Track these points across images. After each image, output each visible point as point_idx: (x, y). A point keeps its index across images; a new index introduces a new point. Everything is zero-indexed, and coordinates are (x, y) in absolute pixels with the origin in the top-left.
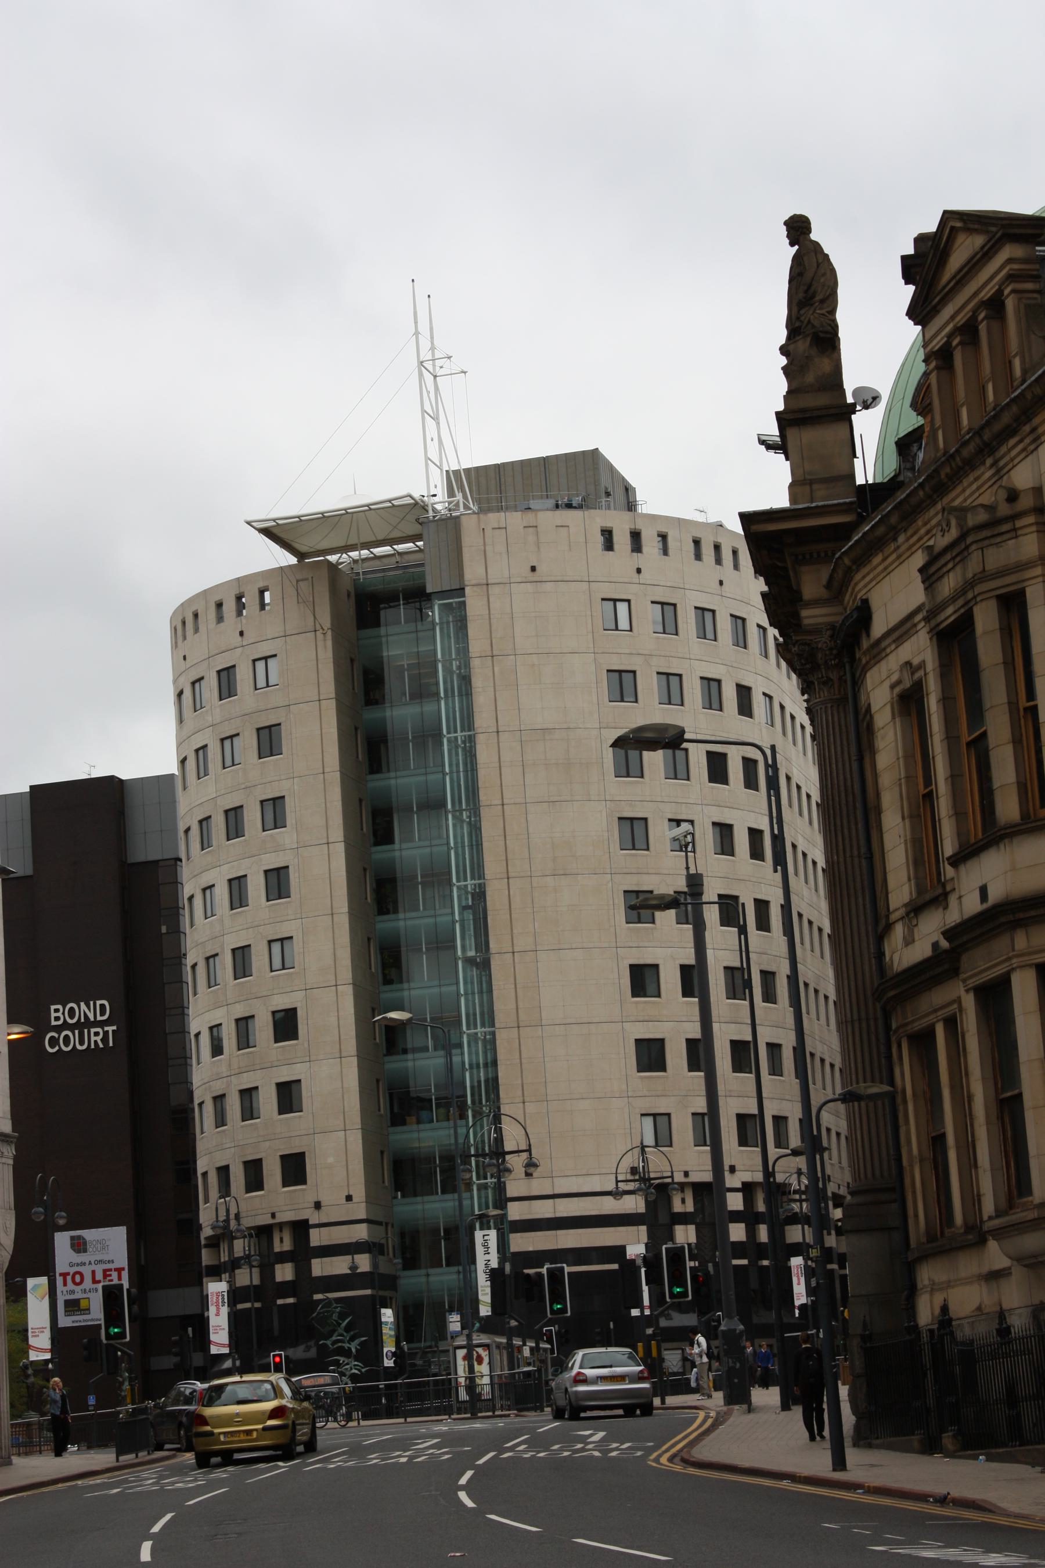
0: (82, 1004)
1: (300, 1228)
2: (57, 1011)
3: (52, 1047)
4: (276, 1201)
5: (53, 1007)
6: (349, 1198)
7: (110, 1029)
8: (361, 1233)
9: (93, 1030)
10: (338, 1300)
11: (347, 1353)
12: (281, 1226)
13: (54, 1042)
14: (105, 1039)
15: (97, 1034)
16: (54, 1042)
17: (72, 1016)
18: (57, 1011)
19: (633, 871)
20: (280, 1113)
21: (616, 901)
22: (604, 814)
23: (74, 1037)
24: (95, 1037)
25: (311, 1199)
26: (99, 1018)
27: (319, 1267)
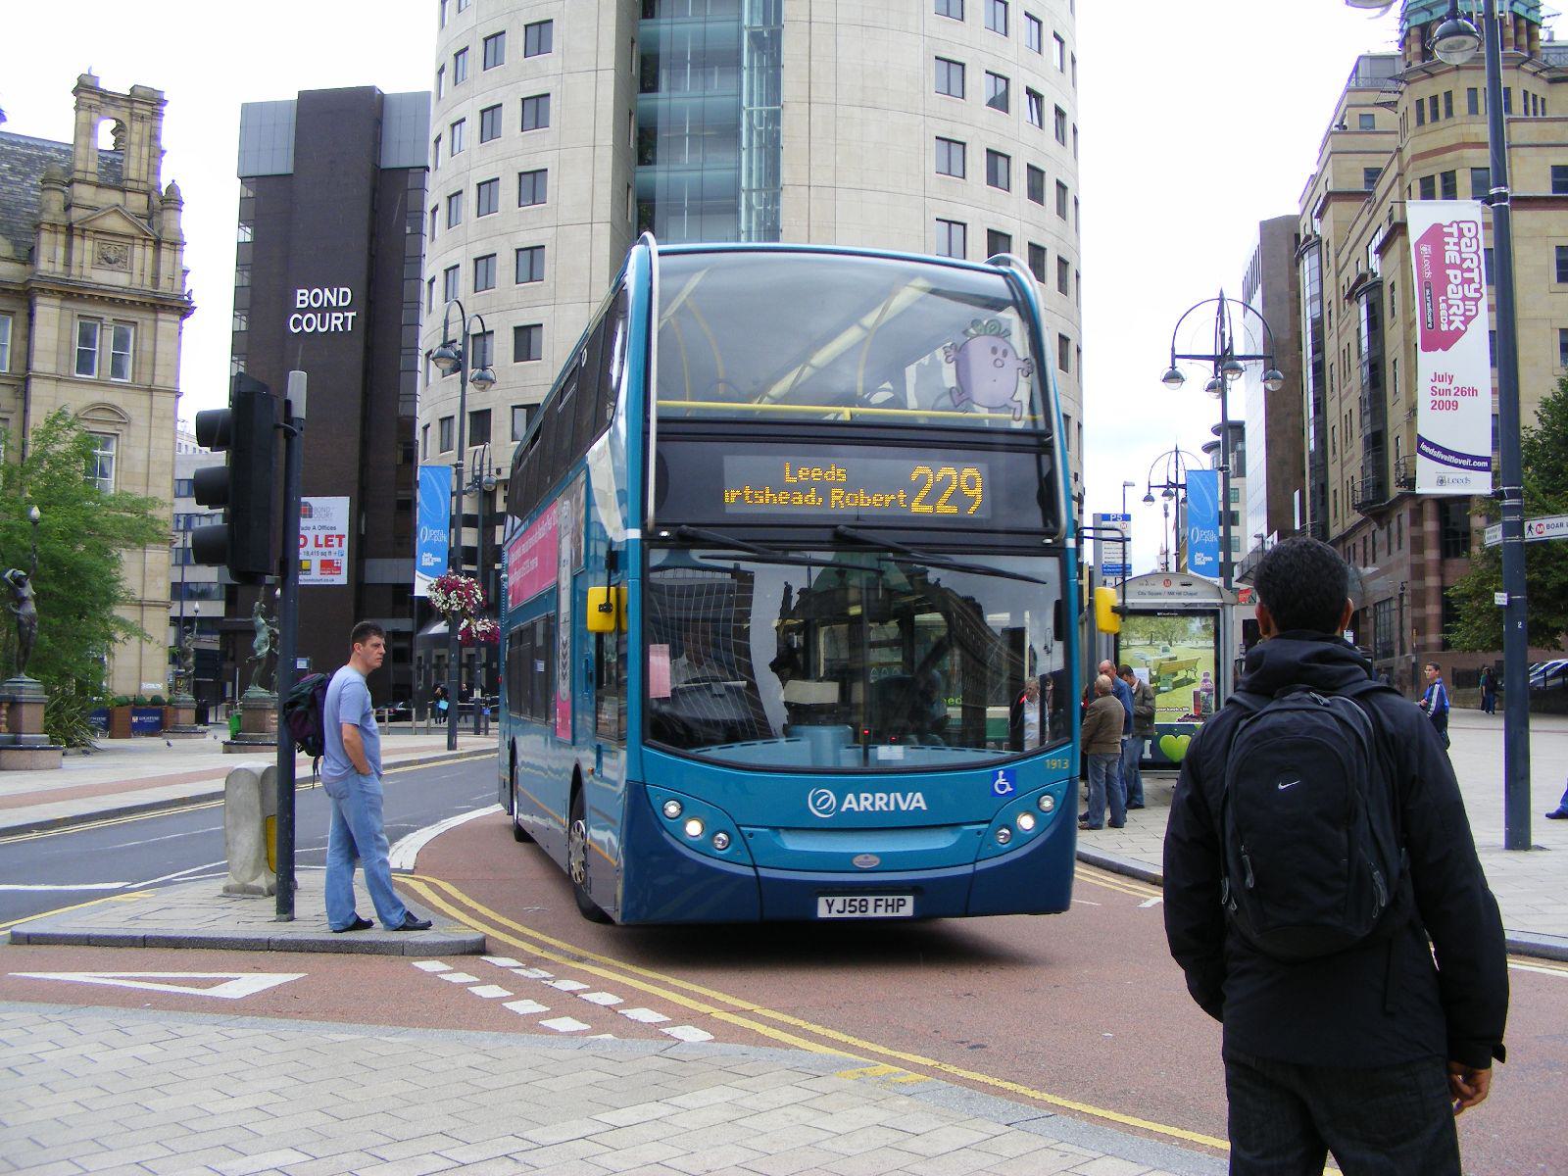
0: (327, 290)
5: (299, 291)
7: (350, 315)
9: (334, 315)
13: (297, 323)
15: (337, 318)
16: (297, 323)
18: (302, 295)
19: (947, 117)
20: (516, 360)
21: (927, 146)
22: (921, 50)
24: (335, 321)
26: (341, 304)
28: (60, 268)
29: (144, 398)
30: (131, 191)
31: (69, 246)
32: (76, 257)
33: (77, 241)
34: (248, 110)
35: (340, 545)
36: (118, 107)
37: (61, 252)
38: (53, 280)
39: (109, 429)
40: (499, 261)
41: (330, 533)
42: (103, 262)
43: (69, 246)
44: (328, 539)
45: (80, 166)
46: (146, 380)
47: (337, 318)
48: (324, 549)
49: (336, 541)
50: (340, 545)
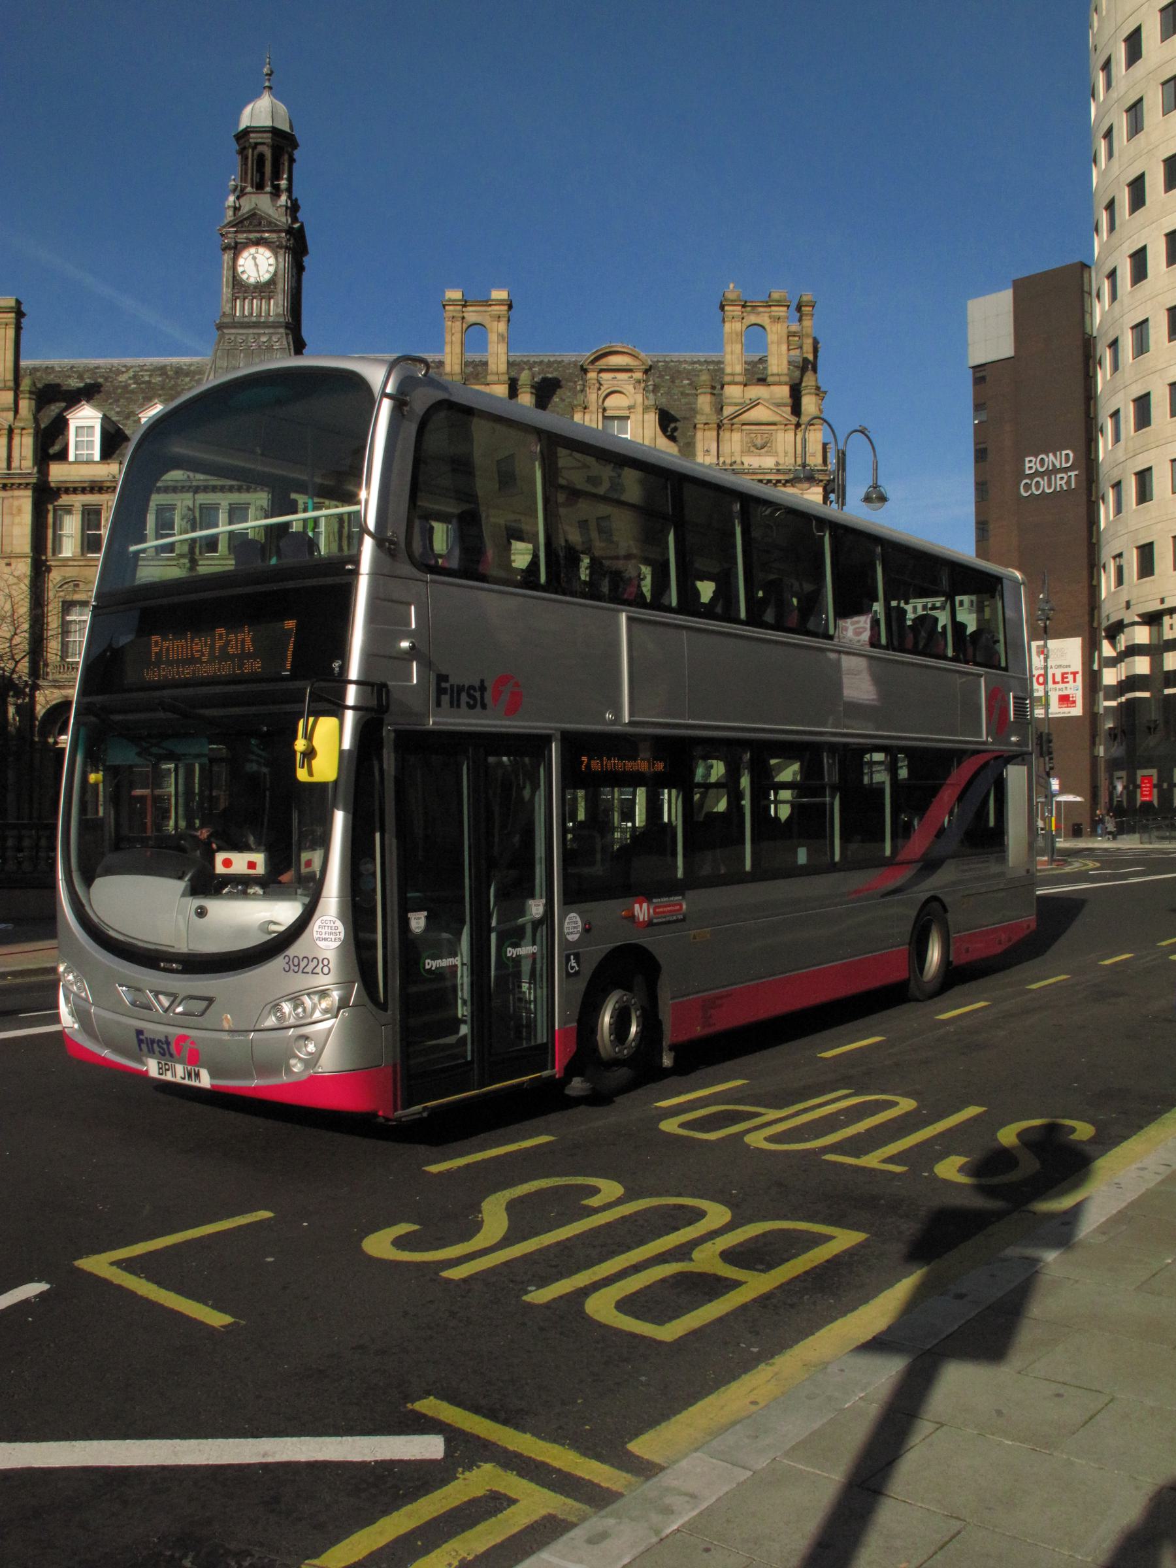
0: (1051, 455)
2: (1030, 461)
3: (1026, 491)
5: (1027, 459)
7: (1072, 474)
9: (1059, 476)
14: (1068, 483)
15: (1062, 478)
17: (1042, 466)
18: (1030, 461)
23: (1044, 483)
24: (1060, 482)
26: (1064, 465)
28: (715, 461)
30: (775, 384)
32: (726, 448)
35: (1075, 681)
36: (758, 313)
41: (1065, 670)
42: (752, 449)
44: (1064, 676)
45: (728, 370)
47: (1062, 478)
48: (1061, 686)
49: (1071, 677)
50: (1075, 681)
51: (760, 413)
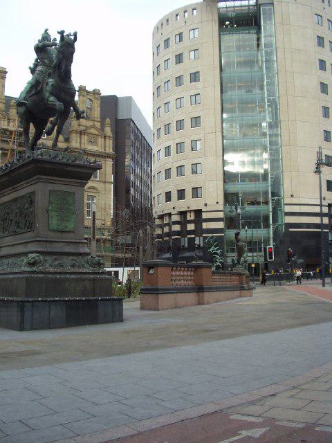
1: (198, 212)
4: (190, 203)
6: (217, 203)
8: (221, 215)
10: (216, 236)
11: (217, 254)
12: (190, 211)
25: (204, 202)
27: (205, 226)
29: (103, 185)
31: (80, 138)
32: (83, 142)
33: (83, 136)
34: (130, 98)
37: (79, 139)
38: (76, 148)
39: (94, 194)
40: (186, 145)
43: (80, 138)
46: (103, 180)
51: (93, 131)
